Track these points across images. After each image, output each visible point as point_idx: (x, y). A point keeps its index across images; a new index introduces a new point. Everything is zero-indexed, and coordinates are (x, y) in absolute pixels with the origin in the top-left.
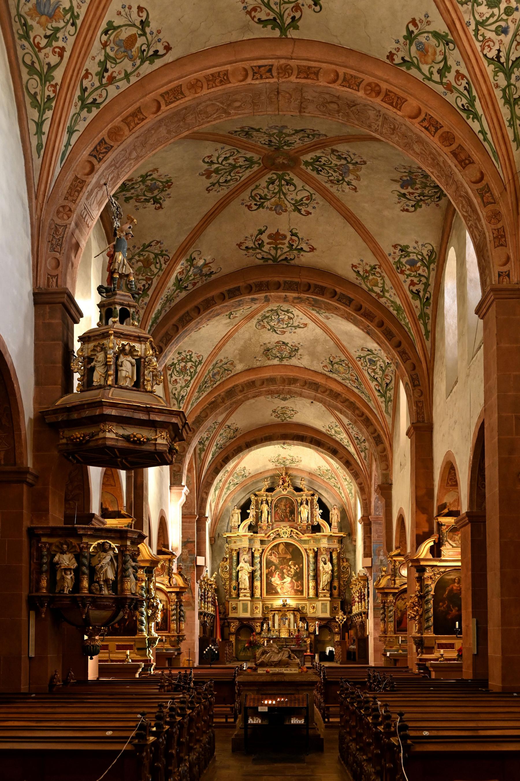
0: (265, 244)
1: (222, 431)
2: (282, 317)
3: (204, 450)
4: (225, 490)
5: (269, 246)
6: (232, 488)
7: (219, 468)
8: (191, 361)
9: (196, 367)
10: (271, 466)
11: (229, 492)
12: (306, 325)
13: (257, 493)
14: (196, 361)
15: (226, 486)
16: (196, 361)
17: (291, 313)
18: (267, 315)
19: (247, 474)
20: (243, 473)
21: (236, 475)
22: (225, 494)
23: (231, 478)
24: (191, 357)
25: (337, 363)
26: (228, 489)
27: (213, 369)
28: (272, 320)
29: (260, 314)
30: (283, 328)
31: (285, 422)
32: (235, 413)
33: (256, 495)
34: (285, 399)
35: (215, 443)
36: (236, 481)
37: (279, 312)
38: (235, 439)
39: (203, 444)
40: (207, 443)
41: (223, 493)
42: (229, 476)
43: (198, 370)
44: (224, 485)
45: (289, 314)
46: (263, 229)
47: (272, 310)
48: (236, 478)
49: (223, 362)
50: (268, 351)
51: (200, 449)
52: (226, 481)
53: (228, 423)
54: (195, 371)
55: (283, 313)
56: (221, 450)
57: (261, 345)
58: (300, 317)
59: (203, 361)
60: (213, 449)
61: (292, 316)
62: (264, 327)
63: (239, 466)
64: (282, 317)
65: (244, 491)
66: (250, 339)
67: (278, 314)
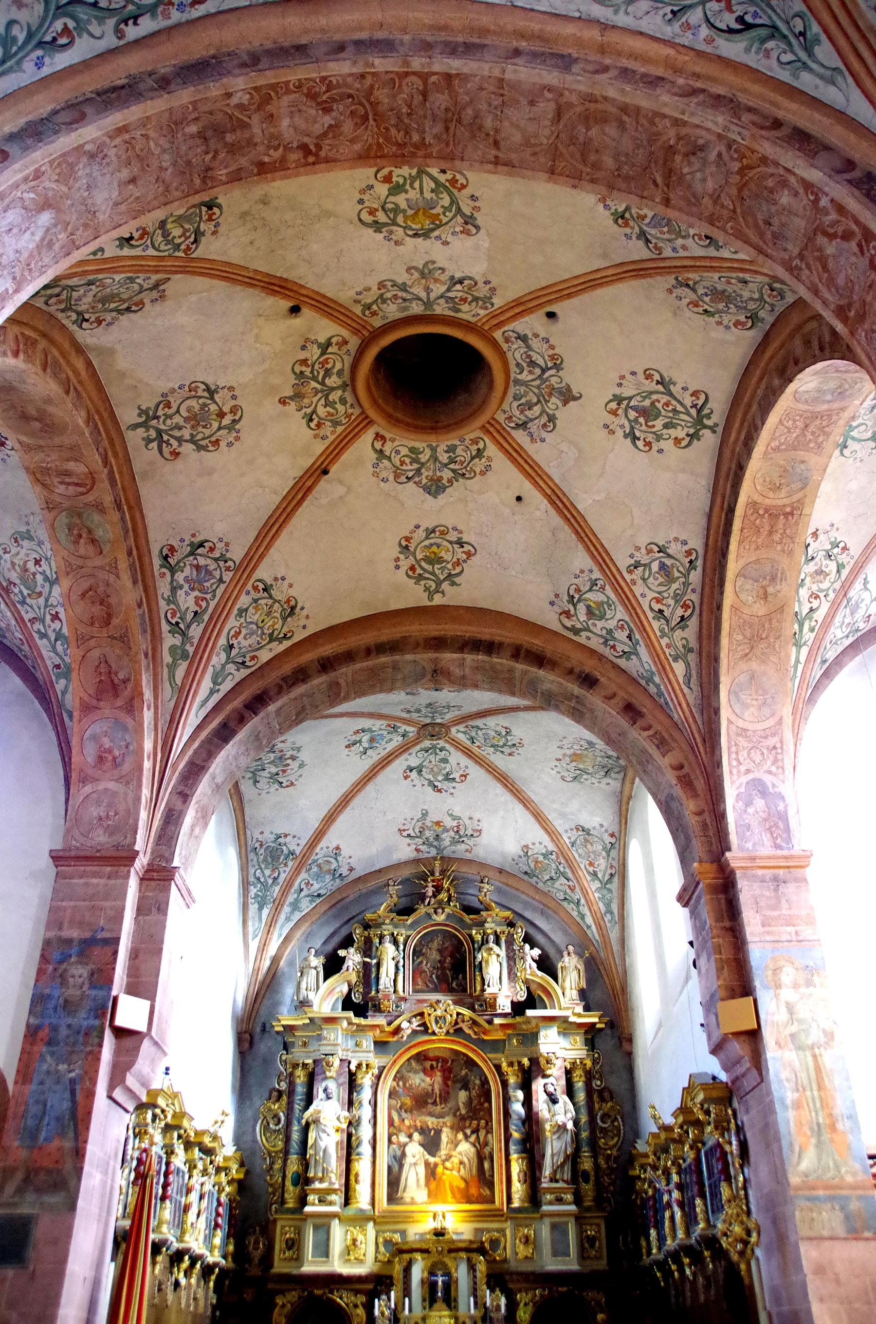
1: (244, 601)
3: (185, 656)
4: (286, 909)
6: (306, 906)
7: (232, 724)
10: (405, 851)
11: (297, 916)
13: (369, 916)
15: (291, 898)
19: (345, 872)
20: (334, 865)
21: (315, 869)
22: (288, 919)
23: (303, 875)
26: (295, 906)
31: (438, 600)
32: (284, 534)
33: (366, 926)
34: (435, 488)
35: (222, 641)
36: (316, 886)
38: (287, 644)
39: (183, 634)
40: (196, 631)
41: (282, 917)
42: (297, 871)
44: (284, 893)
48: (318, 877)
51: (173, 649)
52: (289, 883)
53: (264, 572)
56: (244, 672)
60: (218, 659)
63: (323, 844)
65: (335, 917)
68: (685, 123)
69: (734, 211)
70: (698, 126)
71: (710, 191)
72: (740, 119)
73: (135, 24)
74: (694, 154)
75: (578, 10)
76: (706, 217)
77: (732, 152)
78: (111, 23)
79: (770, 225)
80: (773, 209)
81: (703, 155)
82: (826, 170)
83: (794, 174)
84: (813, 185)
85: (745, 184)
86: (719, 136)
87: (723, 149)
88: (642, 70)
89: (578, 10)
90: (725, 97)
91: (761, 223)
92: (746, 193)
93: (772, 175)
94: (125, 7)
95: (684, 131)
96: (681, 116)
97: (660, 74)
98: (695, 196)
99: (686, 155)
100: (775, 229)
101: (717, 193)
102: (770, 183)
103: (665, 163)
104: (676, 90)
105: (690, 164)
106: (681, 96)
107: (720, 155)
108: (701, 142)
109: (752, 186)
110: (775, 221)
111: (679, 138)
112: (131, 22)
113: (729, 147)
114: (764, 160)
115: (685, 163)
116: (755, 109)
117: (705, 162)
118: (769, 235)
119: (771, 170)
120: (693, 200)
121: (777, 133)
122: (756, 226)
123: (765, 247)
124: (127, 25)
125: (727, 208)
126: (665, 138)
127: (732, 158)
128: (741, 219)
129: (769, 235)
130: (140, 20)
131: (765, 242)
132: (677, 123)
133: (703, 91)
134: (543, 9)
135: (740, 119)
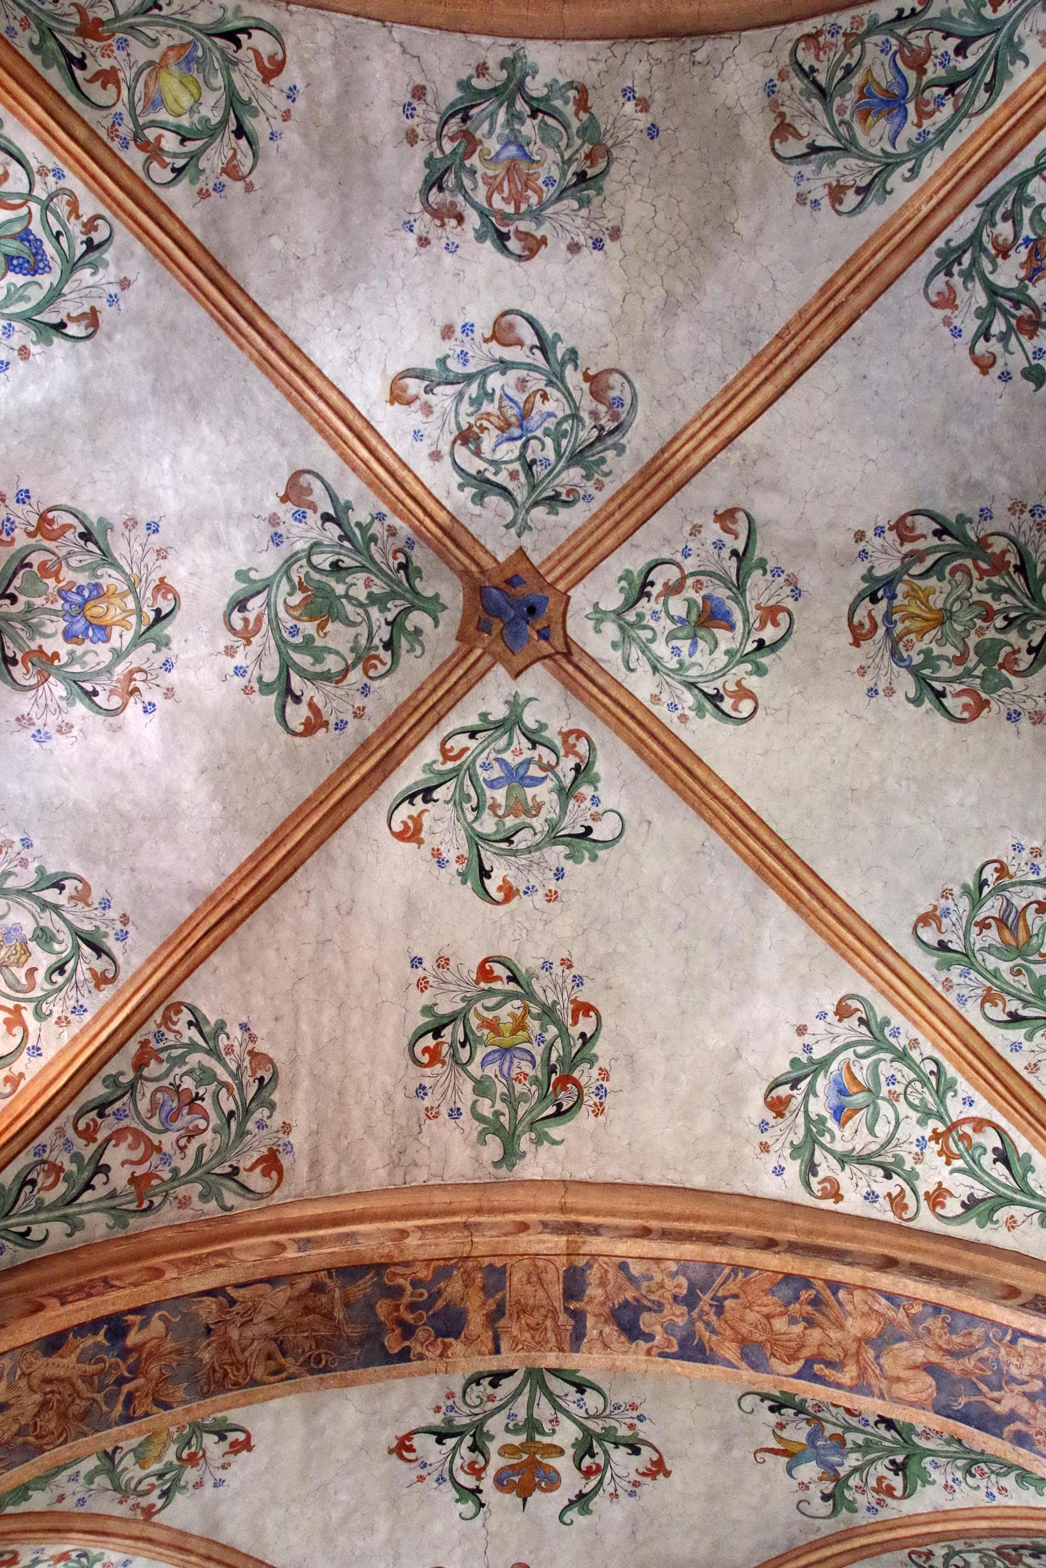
0: (570, 1452)
2: (509, 451)
5: (555, 1440)
8: (992, 291)
9: (974, 240)
12: (397, 396)
14: (967, 276)
16: (967, 276)
17: (468, 479)
18: (574, 474)
24: (984, 314)
25: (211, 133)
27: (889, 164)
28: (557, 436)
29: (612, 487)
30: (504, 366)
37: (521, 494)
43: (973, 213)
45: (473, 465)
46: (572, 1515)
47: (554, 501)
49: (830, 174)
50: (582, 177)
54: (988, 220)
55: (502, 478)
57: (615, 234)
58: (424, 448)
59: (929, 260)
61: (463, 454)
62: (597, 384)
64: (509, 451)
66: (670, 307)
67: (529, 466)
73: (901, 11)
75: (291, 13)
78: (933, 12)
89: (291, 13)
94: (910, 32)
112: (907, 13)
124: (913, 10)
130: (894, 14)
134: (339, 15)
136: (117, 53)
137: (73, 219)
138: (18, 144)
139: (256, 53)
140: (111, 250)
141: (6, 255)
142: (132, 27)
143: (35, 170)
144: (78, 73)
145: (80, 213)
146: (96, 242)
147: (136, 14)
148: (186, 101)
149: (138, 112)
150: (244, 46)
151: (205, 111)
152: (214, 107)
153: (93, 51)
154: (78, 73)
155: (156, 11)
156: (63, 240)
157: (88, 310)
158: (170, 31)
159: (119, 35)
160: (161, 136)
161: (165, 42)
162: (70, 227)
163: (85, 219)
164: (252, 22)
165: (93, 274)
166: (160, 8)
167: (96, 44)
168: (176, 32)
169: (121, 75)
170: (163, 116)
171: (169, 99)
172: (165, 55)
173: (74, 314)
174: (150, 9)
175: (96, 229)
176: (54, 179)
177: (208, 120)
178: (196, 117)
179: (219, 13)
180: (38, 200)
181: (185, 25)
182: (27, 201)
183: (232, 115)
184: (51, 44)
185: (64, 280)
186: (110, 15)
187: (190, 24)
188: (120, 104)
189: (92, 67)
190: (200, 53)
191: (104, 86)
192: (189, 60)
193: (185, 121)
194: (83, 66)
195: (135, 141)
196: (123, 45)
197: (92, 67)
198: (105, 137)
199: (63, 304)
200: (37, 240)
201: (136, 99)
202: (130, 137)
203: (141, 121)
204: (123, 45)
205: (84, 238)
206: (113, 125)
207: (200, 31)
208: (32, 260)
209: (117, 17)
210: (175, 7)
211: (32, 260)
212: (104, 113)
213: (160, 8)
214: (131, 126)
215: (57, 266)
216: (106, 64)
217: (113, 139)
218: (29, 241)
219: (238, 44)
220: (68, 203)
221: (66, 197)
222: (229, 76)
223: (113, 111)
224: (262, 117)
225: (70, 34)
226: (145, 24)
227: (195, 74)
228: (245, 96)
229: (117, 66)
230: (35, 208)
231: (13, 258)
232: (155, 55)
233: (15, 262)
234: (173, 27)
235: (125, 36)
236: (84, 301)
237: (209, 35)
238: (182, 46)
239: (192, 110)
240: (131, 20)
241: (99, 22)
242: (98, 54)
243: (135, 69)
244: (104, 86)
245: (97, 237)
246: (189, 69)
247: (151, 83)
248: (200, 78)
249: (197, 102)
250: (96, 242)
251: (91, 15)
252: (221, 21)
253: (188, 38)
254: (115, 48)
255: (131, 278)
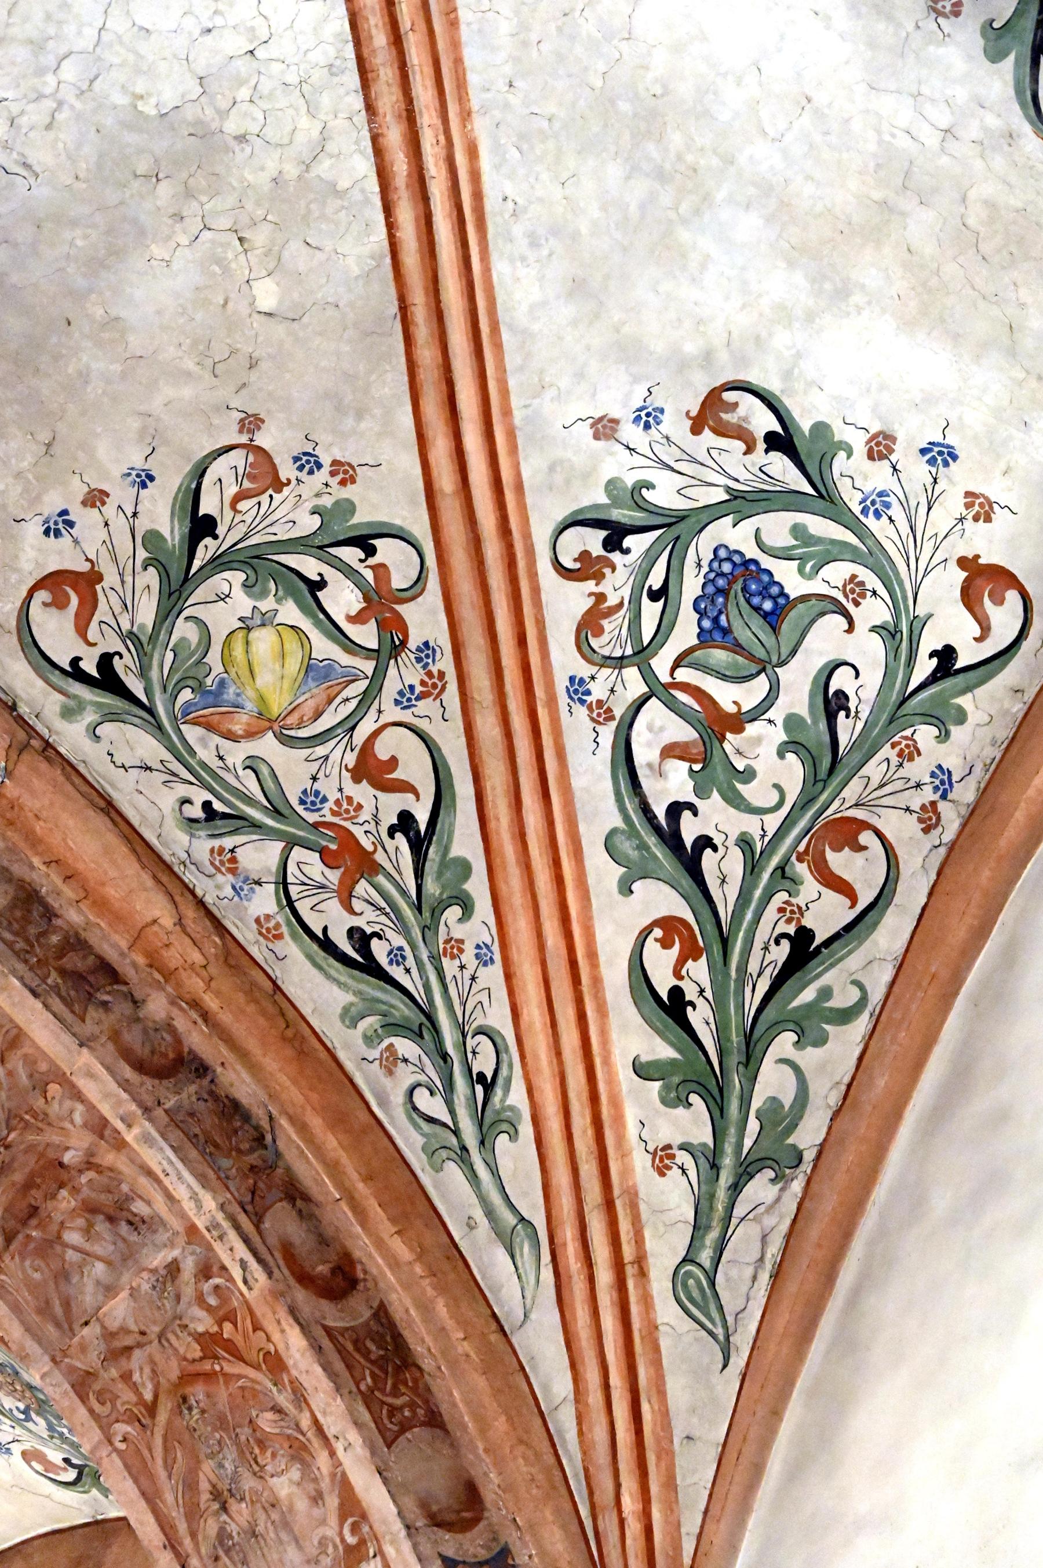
68: (120, 1145)
69: (152, 1409)
70: (149, 1173)
71: (114, 1325)
72: (258, 1221)
74: (111, 1219)
76: (72, 1370)
77: (207, 1286)
79: (224, 1508)
80: (248, 1483)
81: (134, 1237)
82: (409, 1503)
83: (332, 1454)
84: (364, 1516)
85: (209, 1377)
86: (192, 1230)
87: (189, 1266)
88: (73, 916)
90: (246, 1117)
91: (204, 1486)
92: (198, 1392)
93: (278, 1410)
95: (108, 1158)
96: (120, 1126)
97: (111, 955)
98: (67, 1304)
99: (91, 1209)
100: (233, 1528)
101: (128, 1341)
102: (267, 1422)
103: (29, 1185)
104: (132, 1037)
105: (88, 1231)
106: (140, 1067)
107: (173, 1269)
108: (139, 1207)
109: (222, 1394)
110: (241, 1511)
111: (89, 1164)
113: (205, 1272)
114: (275, 1364)
115: (80, 1222)
116: (307, 1198)
117: (128, 1256)
118: (211, 1527)
119: (283, 1399)
120: (58, 1310)
121: (334, 1316)
122: (191, 1486)
123: (187, 1542)
125: (135, 1388)
126: (56, 1139)
127: (200, 1300)
128: (158, 1442)
129: (211, 1527)
131: (193, 1535)
132: (100, 1127)
133: (202, 1069)
135: (258, 1221)
136: (333, 796)
137: (612, 601)
138: (608, 784)
139: (82, 630)
140: (586, 502)
141: (775, 629)
142: (276, 813)
143: (614, 724)
144: (422, 817)
145: (591, 601)
146: (603, 534)
147: (256, 826)
148: (264, 641)
149: (362, 685)
150: (97, 652)
151: (242, 603)
152: (223, 598)
153: (371, 827)
154: (422, 817)
155: (218, 806)
156: (656, 580)
157: (707, 433)
158: (214, 763)
159: (312, 818)
160: (352, 619)
161: (237, 754)
162: (626, 592)
163: (590, 586)
164: (56, 677)
165: (650, 486)
166: (207, 806)
167: (358, 832)
168: (205, 754)
169: (351, 759)
170: (324, 647)
171: (294, 664)
172: (251, 734)
173: (740, 446)
174: (225, 816)
175: (584, 556)
176: (592, 686)
177: (246, 586)
178: (267, 604)
179: (107, 729)
180: (648, 674)
181: (183, 753)
182: (666, 687)
183: (197, 564)
184: (431, 887)
185: (712, 513)
186: (298, 854)
187: (171, 749)
188: (385, 719)
189: (391, 805)
190: (186, 695)
191: (393, 763)
192: (214, 696)
193: (290, 613)
194: (406, 820)
195: (404, 643)
196: (312, 799)
197: (391, 805)
198: (452, 687)
199: (743, 475)
200: (702, 614)
201: (354, 703)
202: (407, 658)
203: (368, 667)
204: (312, 799)
205: (616, 557)
206: (422, 696)
207: (160, 727)
208: (738, 586)
209: (291, 843)
210: (182, 790)
211: (738, 586)
212: (423, 724)
213: (207, 806)
214: (392, 671)
215: (704, 545)
216: (363, 793)
217: (442, 675)
218: (716, 620)
219: (106, 661)
220: (599, 632)
221: (594, 643)
222: (157, 625)
223: (406, 716)
224: (143, 525)
225: (389, 876)
226: (249, 800)
227: (218, 668)
228: (151, 577)
229: (346, 775)
230: (661, 664)
231: (765, 615)
232: (268, 746)
233: (768, 605)
234: (204, 765)
235: (300, 809)
236: (702, 456)
237: (151, 711)
238: (209, 727)
239: (266, 620)
240: (270, 822)
241: (327, 858)
242: (365, 815)
243: (321, 751)
244: (393, 763)
245: (593, 540)
246: (222, 684)
247: (308, 709)
248: (214, 658)
249: (247, 626)
250: (603, 534)
251: (334, 877)
252: (111, 716)
253: (192, 733)
254: (330, 804)
255: (585, 430)
